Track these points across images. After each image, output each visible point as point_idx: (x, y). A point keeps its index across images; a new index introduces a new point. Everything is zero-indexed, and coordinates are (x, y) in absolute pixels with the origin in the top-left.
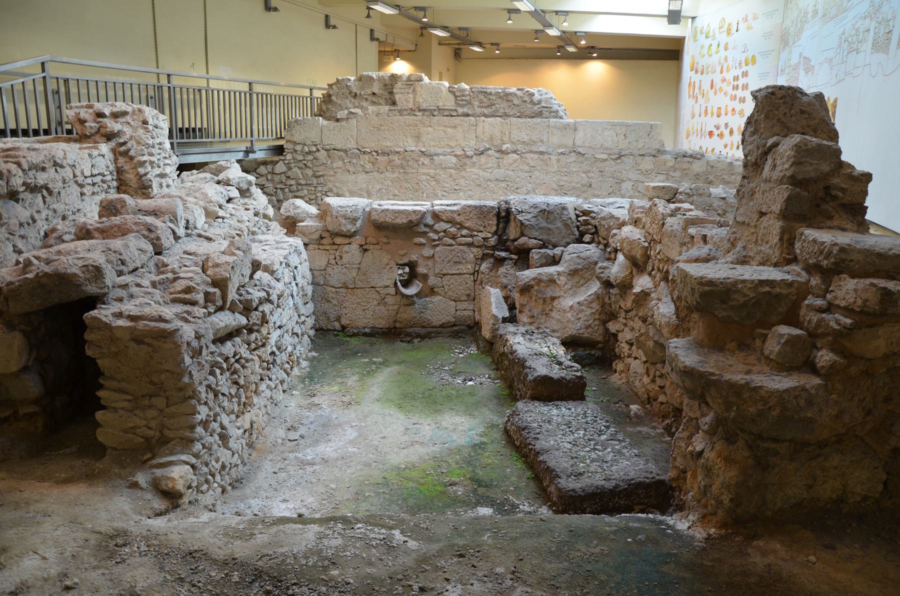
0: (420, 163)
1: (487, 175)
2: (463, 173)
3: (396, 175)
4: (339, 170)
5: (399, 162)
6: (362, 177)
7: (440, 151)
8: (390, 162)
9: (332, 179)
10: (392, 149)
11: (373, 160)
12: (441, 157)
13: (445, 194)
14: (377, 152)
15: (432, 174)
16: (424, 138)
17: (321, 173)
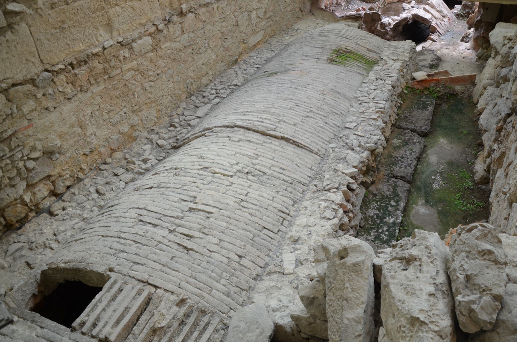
0: (121, 58)
1: (175, 45)
2: (160, 53)
3: (102, 87)
4: (35, 114)
5: (100, 67)
6: (67, 108)
7: (136, 34)
8: (91, 71)
9: (30, 131)
10: (88, 52)
11: (71, 79)
12: (139, 42)
13: (152, 84)
14: (71, 64)
15: (136, 67)
16: (116, 25)
17: (10, 132)
